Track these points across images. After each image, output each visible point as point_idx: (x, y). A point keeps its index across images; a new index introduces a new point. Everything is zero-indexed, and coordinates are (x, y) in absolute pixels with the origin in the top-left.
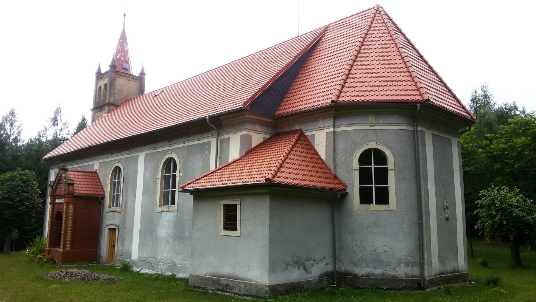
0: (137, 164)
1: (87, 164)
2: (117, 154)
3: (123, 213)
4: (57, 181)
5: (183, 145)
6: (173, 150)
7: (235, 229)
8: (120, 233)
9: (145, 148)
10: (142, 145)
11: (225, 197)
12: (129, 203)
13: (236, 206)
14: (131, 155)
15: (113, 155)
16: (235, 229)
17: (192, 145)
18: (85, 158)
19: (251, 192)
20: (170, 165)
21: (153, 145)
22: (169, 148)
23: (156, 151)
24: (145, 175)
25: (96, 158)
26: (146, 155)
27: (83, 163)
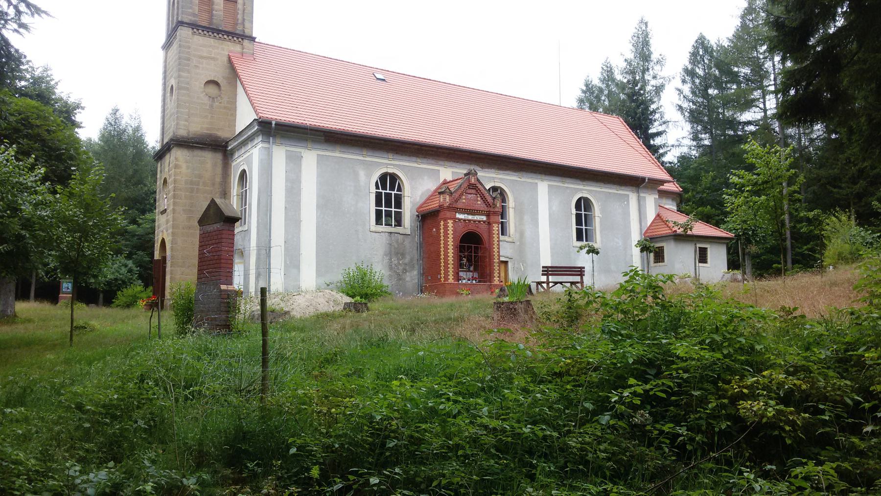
0: (537, 192)
1: (415, 165)
2: (493, 170)
3: (518, 243)
4: (463, 189)
5: (601, 190)
6: (590, 191)
7: (706, 262)
8: (516, 266)
9: (547, 177)
10: (541, 173)
11: (701, 242)
12: (528, 234)
13: (707, 248)
14: (523, 180)
15: (486, 170)
16: (706, 262)
17: (610, 193)
18: (410, 156)
19: (715, 241)
20: (583, 205)
21: (564, 179)
22: (581, 187)
23: (566, 185)
24: (550, 208)
25: (441, 163)
26: (549, 186)
27: (400, 160)
